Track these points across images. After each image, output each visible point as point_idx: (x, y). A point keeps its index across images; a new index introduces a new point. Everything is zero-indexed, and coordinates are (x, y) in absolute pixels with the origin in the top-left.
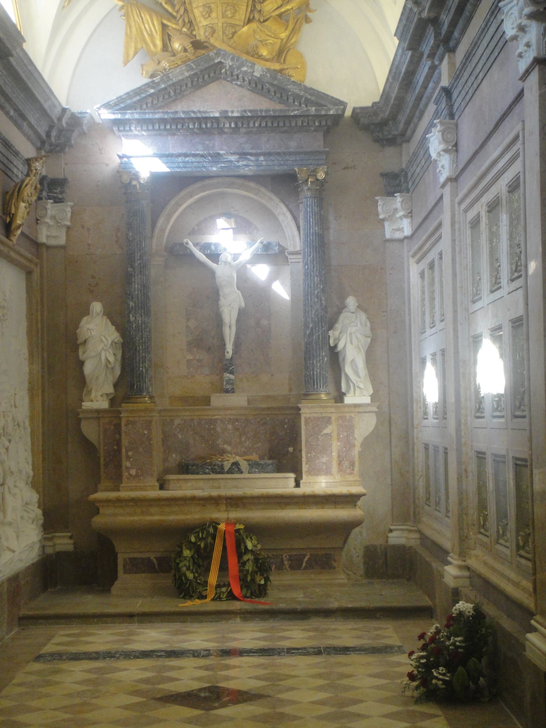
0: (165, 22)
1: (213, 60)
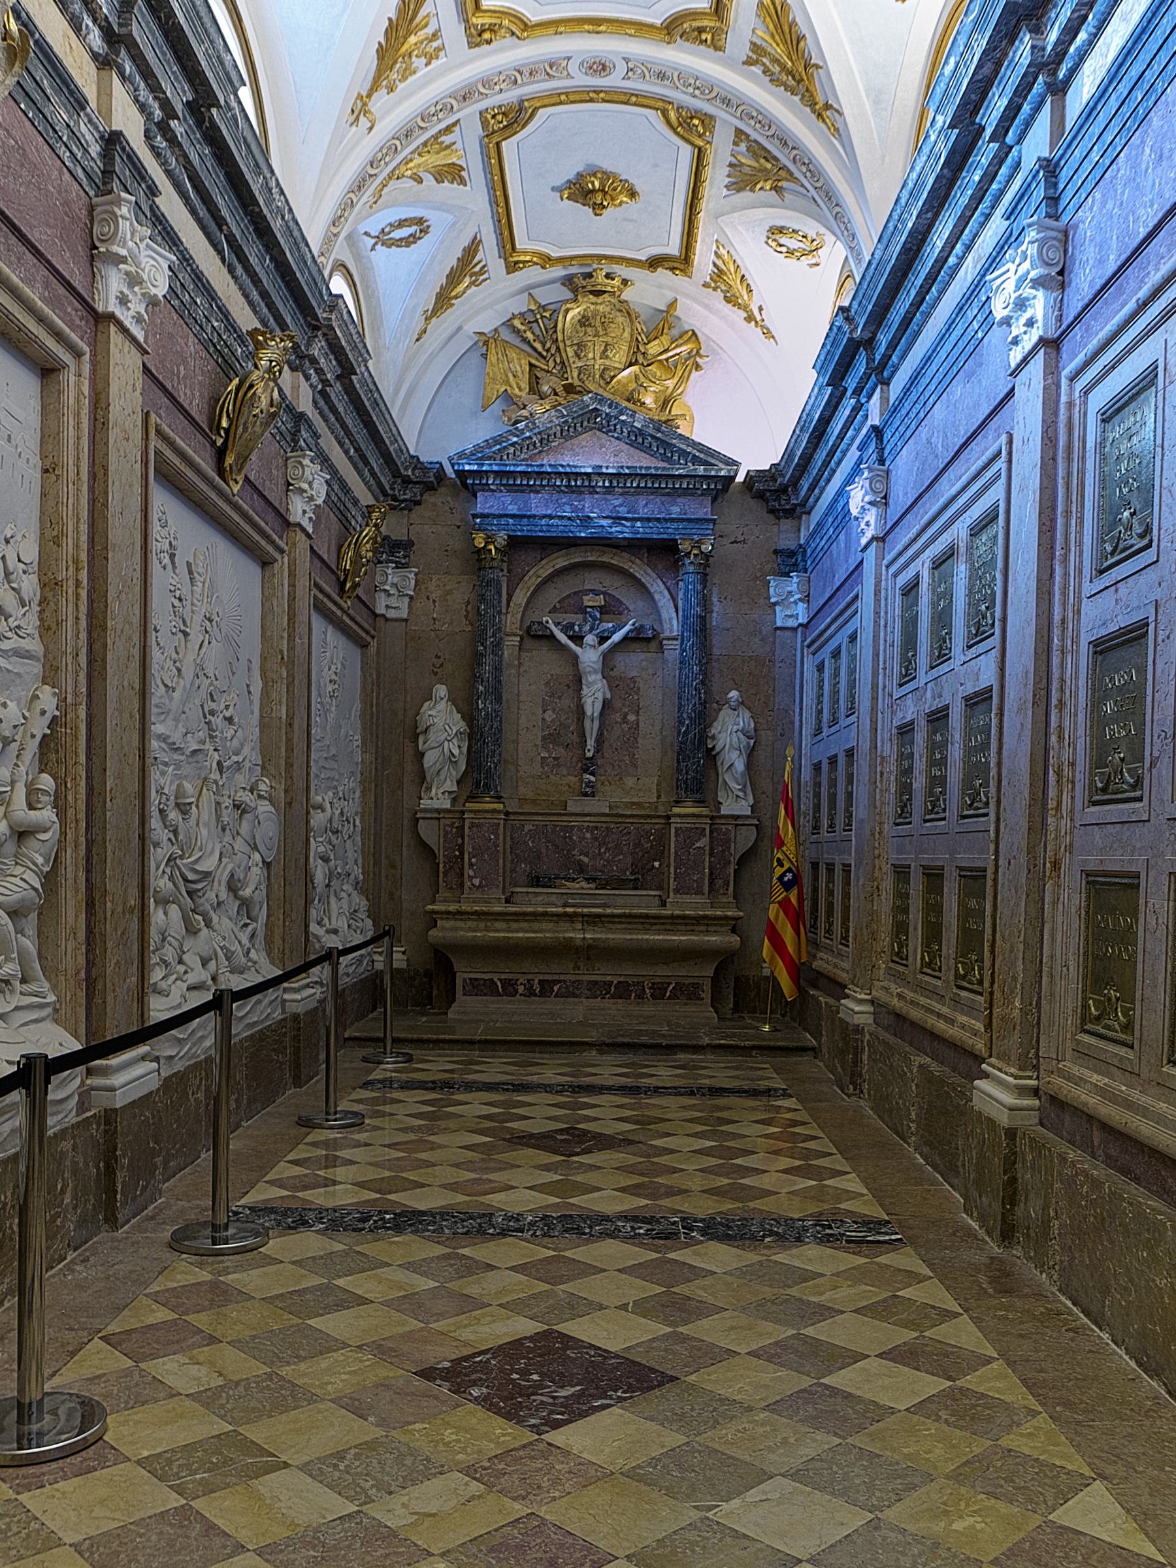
0: (533, 362)
1: (588, 406)
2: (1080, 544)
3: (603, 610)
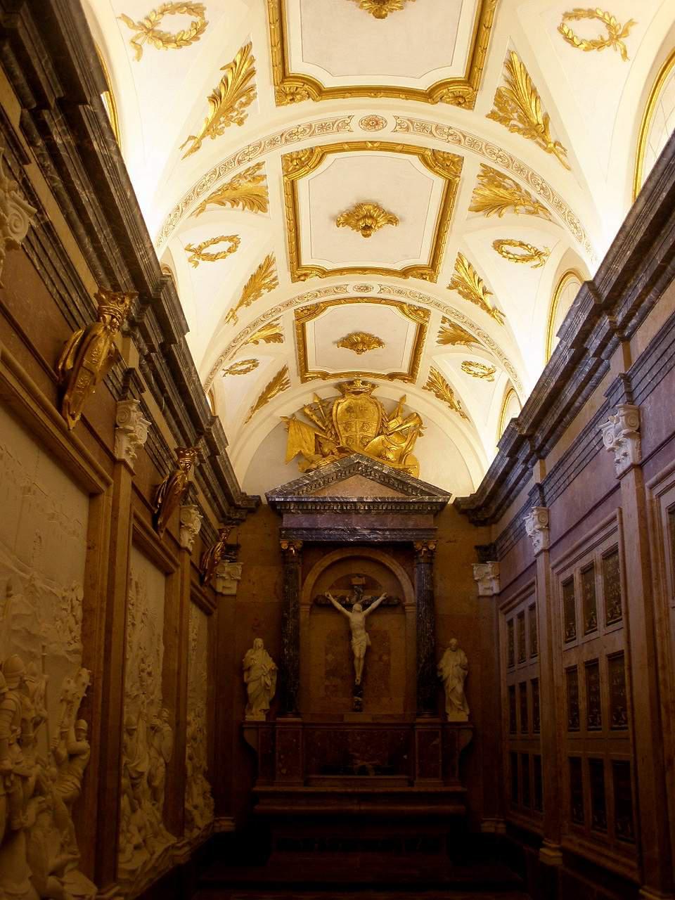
2: (665, 577)
3: (364, 587)
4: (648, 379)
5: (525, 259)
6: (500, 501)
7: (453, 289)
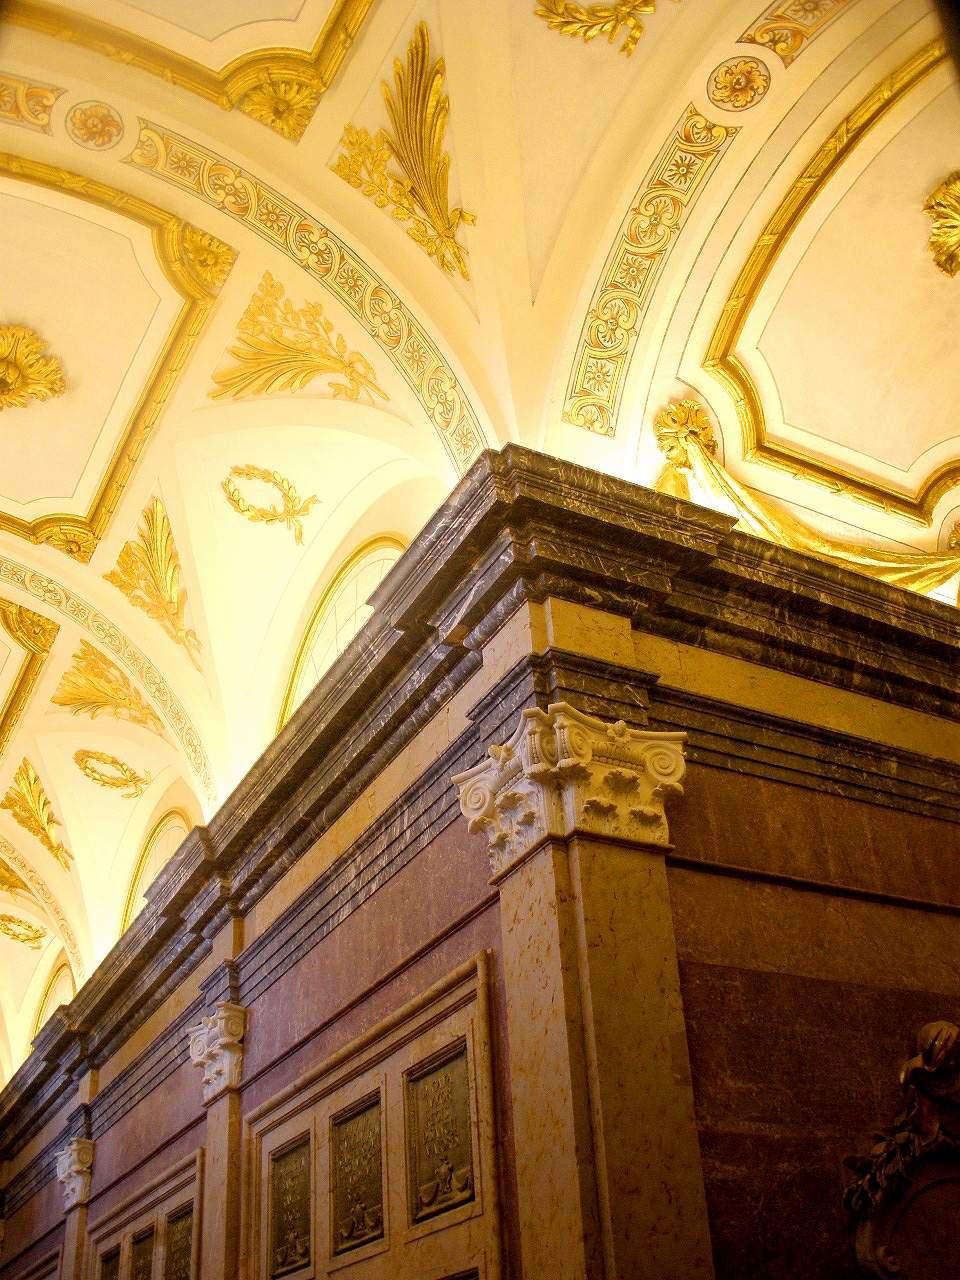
2: (258, 1251)
4: (264, 972)
5: (114, 783)
6: (22, 1125)
7: (6, 808)
